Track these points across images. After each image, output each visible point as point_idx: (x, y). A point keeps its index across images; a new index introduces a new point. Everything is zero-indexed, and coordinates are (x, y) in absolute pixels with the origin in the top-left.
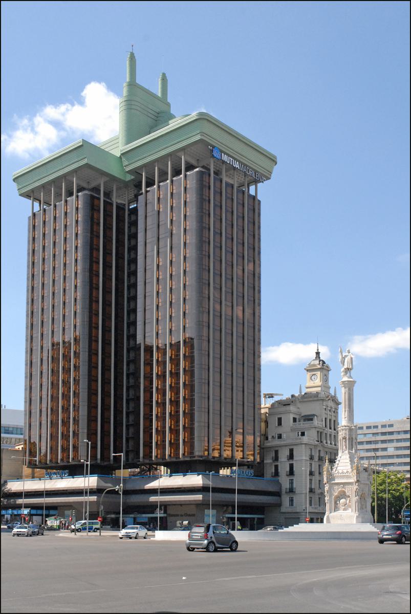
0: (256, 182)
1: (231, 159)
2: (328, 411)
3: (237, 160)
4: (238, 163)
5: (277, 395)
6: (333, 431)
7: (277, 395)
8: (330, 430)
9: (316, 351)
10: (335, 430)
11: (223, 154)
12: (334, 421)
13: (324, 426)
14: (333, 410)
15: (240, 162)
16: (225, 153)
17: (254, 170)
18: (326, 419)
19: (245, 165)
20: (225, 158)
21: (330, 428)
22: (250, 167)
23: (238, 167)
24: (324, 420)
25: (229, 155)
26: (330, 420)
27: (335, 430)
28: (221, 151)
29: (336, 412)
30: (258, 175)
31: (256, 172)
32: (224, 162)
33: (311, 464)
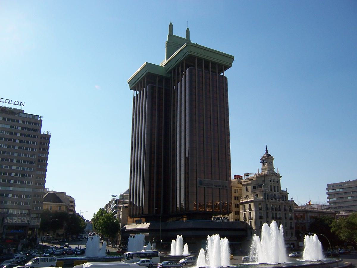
2: (273, 182)
5: (251, 174)
6: (277, 193)
7: (251, 174)
8: (275, 192)
9: (266, 149)
10: (278, 191)
12: (278, 187)
13: (269, 190)
14: (276, 181)
18: (271, 186)
21: (275, 191)
24: (269, 187)
26: (274, 187)
27: (278, 191)
29: (278, 182)
33: (260, 213)
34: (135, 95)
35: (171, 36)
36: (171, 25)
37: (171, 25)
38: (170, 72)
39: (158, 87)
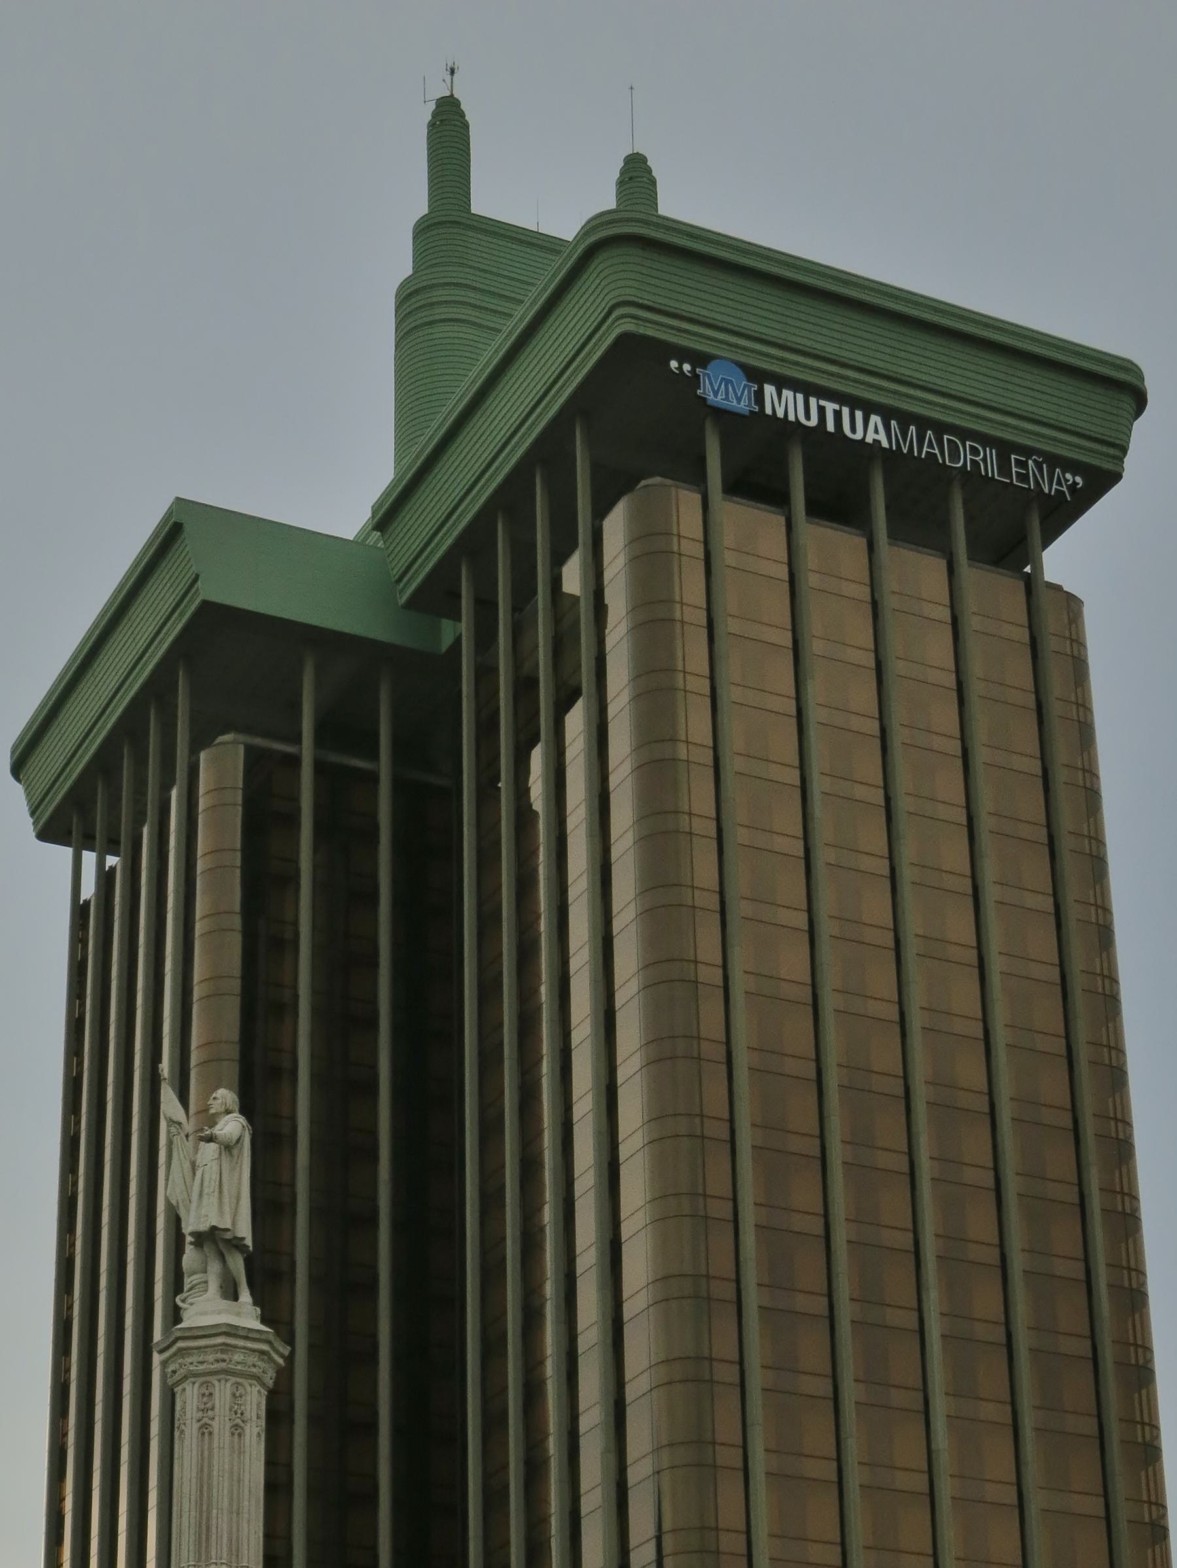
0: (1061, 514)
1: (830, 407)
3: (869, 408)
4: (875, 419)
11: (769, 390)
15: (888, 414)
16: (781, 383)
17: (986, 440)
19: (924, 424)
20: (785, 404)
22: (965, 434)
23: (882, 437)
25: (808, 390)
28: (757, 376)
30: (1023, 465)
31: (1004, 449)
32: (786, 429)
34: (88, 890)
35: (449, 225)
36: (449, 129)
37: (449, 129)
38: (436, 596)
39: (320, 768)
